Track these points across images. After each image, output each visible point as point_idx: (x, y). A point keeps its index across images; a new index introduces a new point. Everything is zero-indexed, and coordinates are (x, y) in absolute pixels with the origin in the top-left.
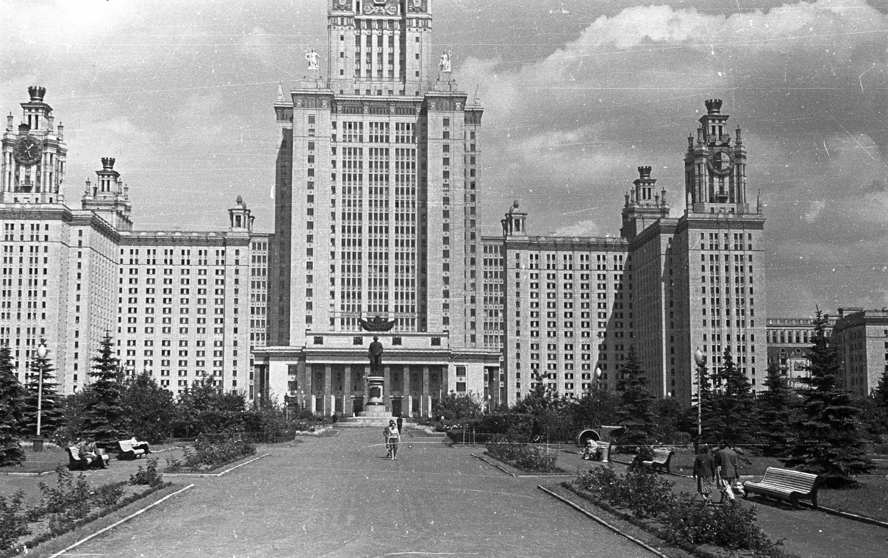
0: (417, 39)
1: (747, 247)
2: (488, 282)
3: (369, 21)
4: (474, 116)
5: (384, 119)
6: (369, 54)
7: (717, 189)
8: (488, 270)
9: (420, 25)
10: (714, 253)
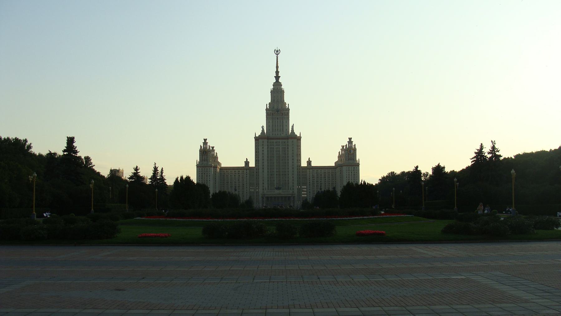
0: (286, 122)
3: (275, 117)
4: (299, 139)
5: (278, 140)
6: (275, 126)
7: (350, 157)
8: (303, 174)
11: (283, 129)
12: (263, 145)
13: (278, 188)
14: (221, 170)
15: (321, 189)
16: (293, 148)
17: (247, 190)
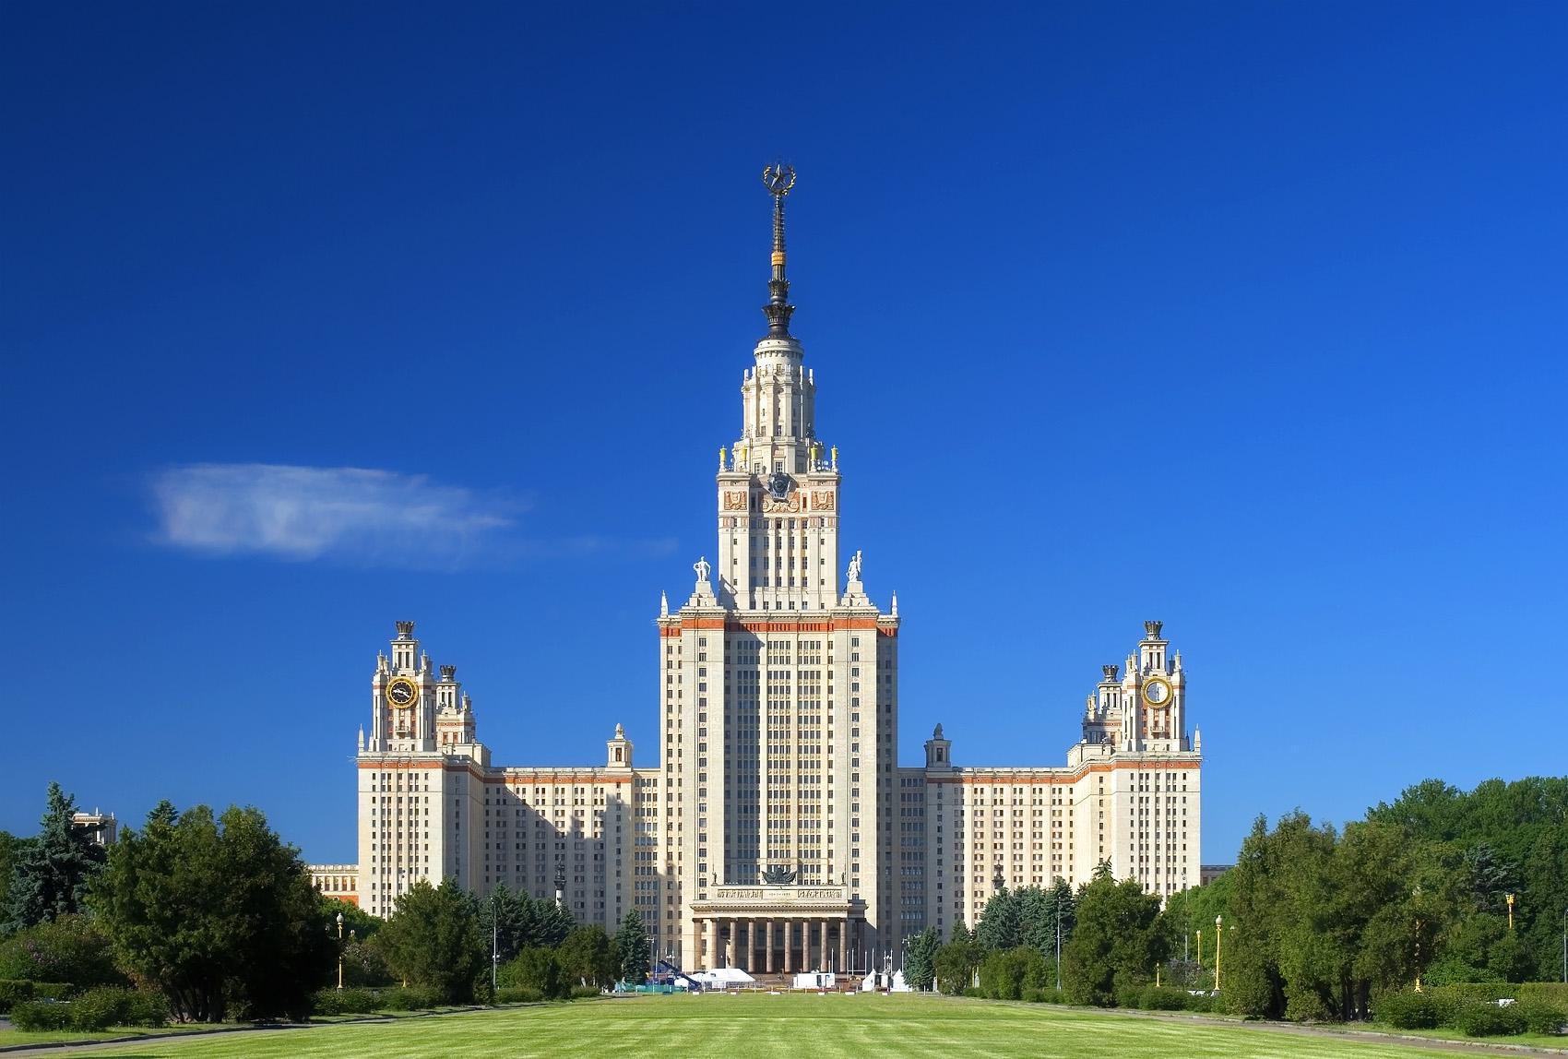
1: (1179, 788)
2: (907, 819)
9: (826, 524)
10: (1144, 794)
11: (804, 581)
12: (702, 657)
13: (779, 877)
14: (488, 785)
15: (998, 882)
17: (619, 886)
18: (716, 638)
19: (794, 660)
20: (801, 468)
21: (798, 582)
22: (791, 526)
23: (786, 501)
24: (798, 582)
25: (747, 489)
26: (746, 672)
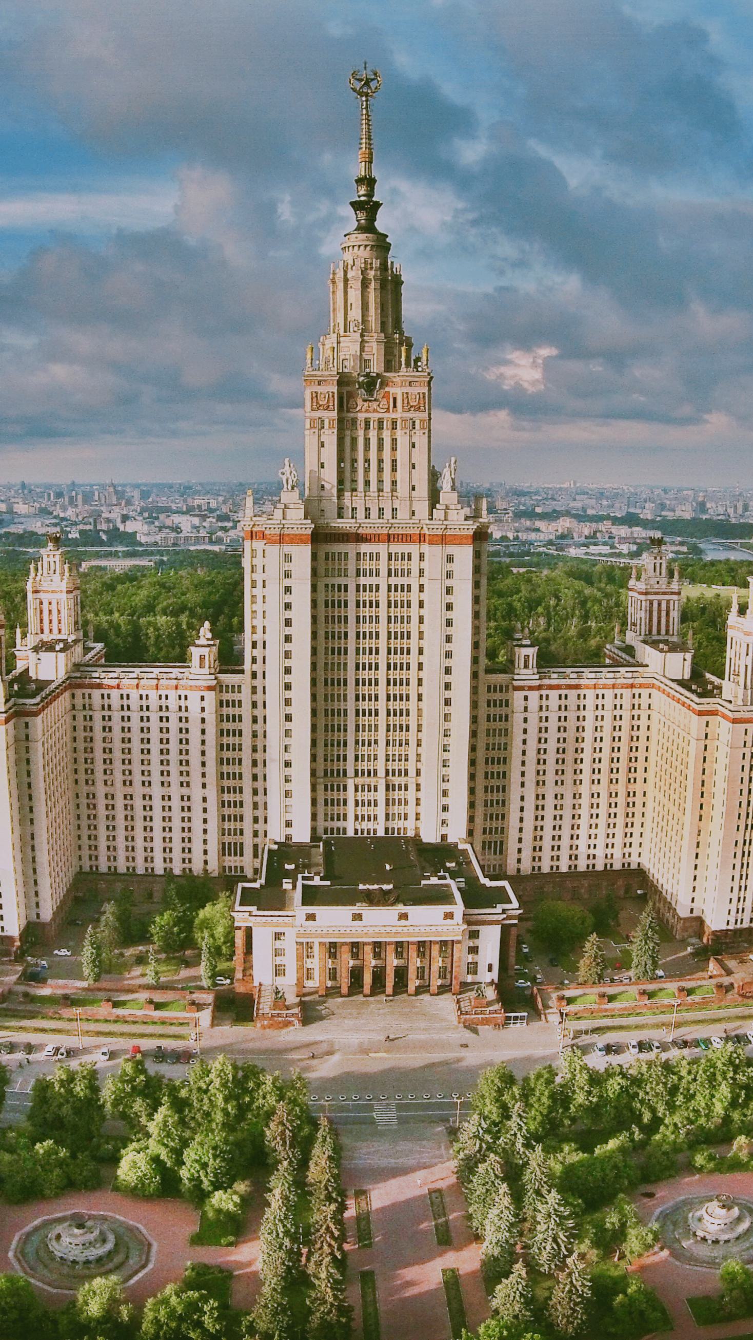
16: (449, 591)
18: (302, 554)
19: (384, 572)
20: (390, 364)
21: (387, 486)
22: (380, 427)
23: (375, 400)
24: (387, 486)
25: (335, 389)
26: (333, 586)
